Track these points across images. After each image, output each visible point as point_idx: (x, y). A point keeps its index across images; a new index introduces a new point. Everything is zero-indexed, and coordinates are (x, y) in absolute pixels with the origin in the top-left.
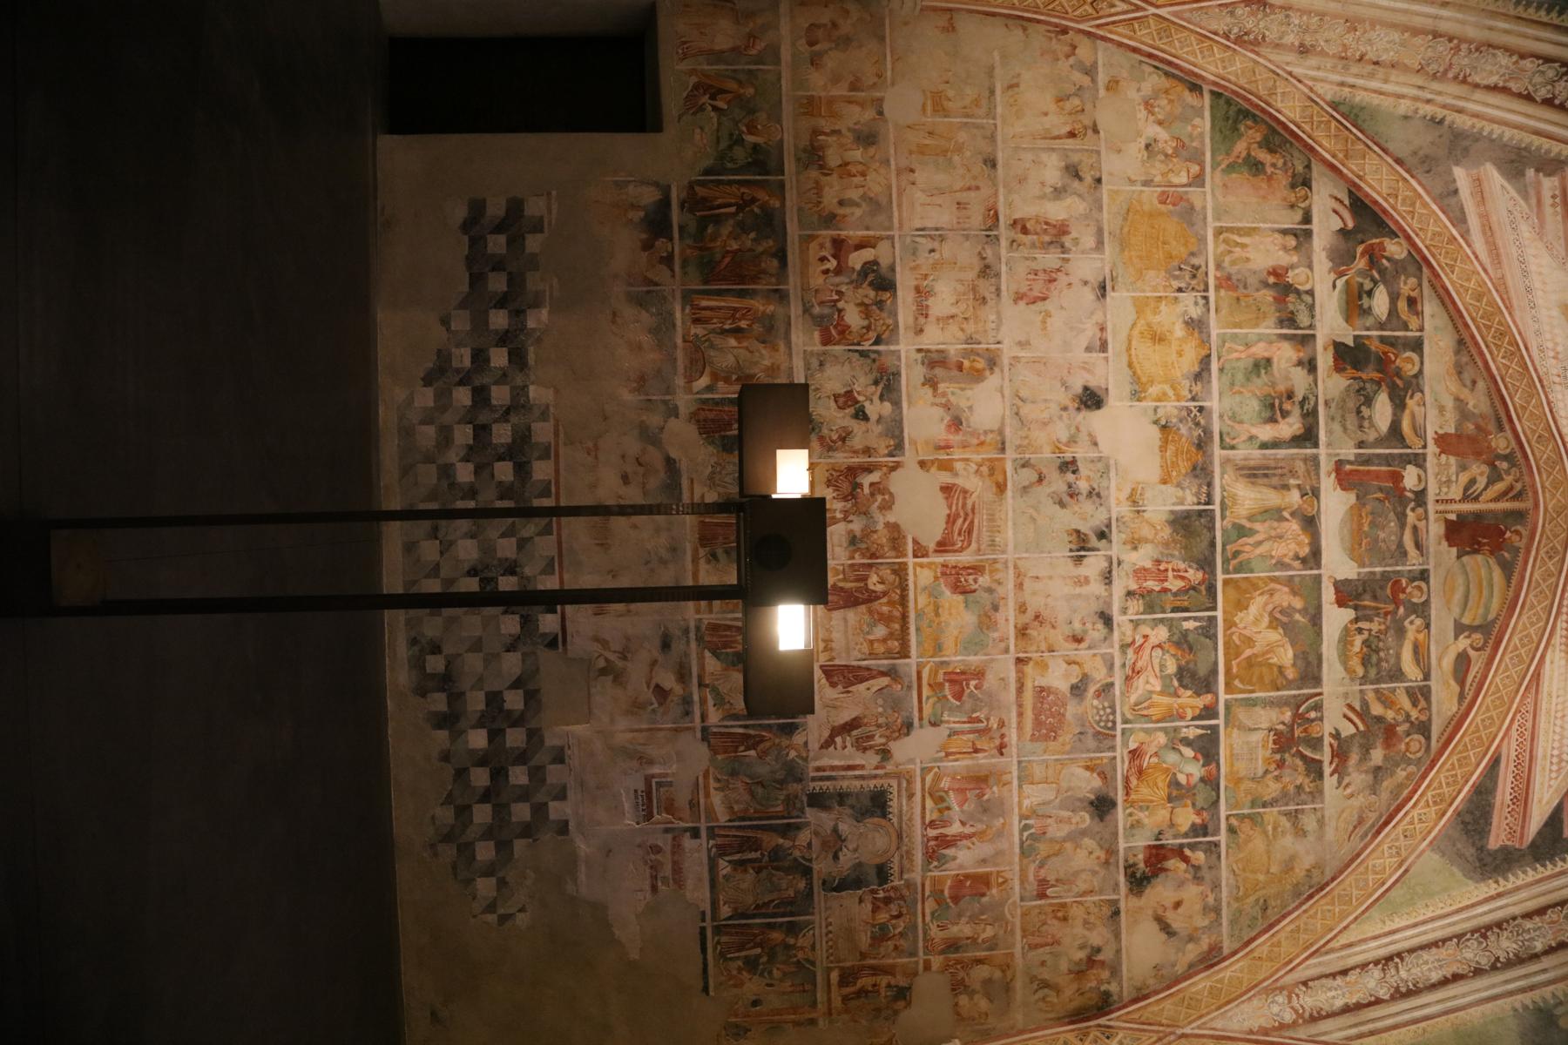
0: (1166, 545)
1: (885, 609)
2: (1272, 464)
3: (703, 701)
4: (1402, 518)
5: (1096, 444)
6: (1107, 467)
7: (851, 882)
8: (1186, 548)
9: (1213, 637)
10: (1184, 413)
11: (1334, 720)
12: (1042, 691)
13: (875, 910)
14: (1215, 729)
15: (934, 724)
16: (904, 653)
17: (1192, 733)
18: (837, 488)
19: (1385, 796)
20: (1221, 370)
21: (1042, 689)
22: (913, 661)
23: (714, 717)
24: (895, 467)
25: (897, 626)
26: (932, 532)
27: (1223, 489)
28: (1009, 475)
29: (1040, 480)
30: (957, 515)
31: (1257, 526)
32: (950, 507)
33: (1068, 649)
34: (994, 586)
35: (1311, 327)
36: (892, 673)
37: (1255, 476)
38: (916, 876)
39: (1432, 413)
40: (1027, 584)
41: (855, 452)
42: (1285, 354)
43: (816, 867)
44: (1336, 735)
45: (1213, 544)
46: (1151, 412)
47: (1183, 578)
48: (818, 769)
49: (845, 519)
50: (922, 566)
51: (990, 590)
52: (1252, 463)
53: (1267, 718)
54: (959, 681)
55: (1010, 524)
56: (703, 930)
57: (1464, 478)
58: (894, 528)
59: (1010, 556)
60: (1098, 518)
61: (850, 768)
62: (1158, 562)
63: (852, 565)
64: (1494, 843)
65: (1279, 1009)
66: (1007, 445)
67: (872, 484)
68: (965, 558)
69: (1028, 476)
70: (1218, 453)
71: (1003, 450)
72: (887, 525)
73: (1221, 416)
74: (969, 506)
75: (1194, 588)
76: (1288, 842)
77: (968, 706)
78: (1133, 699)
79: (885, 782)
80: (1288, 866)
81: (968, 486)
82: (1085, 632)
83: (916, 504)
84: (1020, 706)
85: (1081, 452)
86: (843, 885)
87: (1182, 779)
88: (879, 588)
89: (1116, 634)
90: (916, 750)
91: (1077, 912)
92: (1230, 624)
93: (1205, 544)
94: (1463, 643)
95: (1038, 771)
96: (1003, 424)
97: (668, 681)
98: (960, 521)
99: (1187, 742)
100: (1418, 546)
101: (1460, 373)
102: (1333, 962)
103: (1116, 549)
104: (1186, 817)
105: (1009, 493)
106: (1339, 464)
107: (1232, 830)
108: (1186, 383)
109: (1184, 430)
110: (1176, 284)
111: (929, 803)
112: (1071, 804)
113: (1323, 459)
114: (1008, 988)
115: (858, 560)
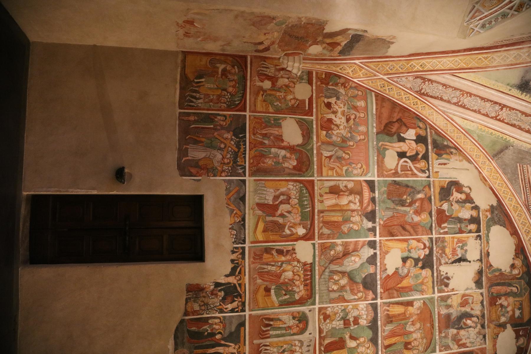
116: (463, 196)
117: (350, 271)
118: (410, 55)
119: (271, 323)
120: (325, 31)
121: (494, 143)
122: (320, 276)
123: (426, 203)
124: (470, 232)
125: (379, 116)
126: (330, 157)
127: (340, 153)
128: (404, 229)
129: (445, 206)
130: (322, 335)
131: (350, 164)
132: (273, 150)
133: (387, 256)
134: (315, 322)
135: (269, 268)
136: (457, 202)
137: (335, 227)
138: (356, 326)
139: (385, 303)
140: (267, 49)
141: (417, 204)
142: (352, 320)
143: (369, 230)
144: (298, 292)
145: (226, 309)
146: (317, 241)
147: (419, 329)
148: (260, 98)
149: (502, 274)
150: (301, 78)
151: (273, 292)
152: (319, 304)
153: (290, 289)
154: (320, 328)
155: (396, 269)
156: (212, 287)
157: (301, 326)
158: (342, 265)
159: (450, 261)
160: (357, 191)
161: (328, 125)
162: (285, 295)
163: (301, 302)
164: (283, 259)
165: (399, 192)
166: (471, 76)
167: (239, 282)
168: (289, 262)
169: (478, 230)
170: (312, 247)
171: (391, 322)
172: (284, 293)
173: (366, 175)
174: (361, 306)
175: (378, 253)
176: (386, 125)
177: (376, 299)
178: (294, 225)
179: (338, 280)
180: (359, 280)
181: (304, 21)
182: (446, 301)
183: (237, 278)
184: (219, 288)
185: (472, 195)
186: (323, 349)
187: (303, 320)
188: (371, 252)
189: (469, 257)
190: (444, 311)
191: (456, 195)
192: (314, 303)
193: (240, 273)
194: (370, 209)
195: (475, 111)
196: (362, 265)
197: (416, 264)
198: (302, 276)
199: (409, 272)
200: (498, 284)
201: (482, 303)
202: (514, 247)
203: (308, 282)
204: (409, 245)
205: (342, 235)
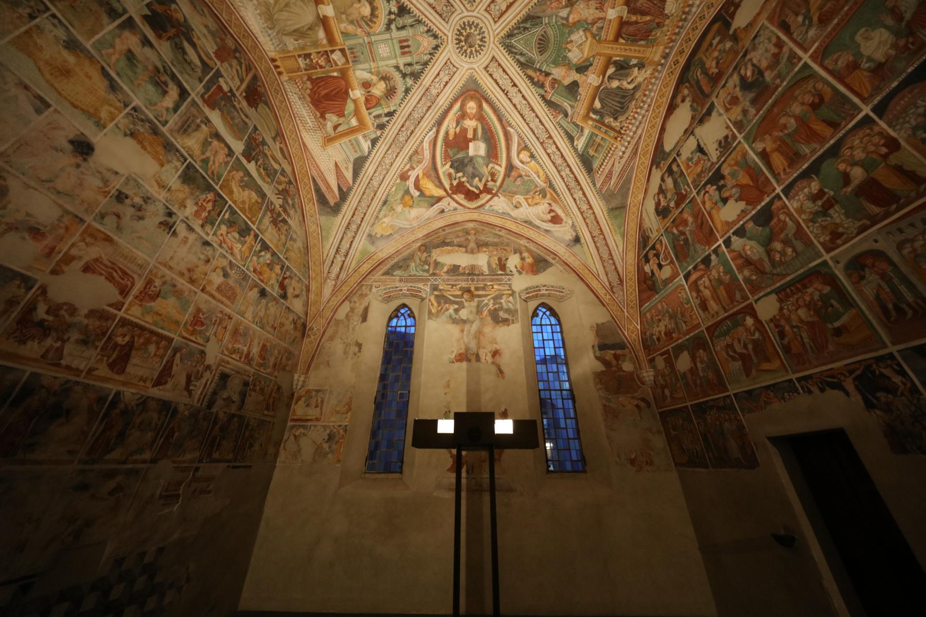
0: (192, 194)
1: (142, 340)
2: (185, 118)
3: (135, 462)
4: (234, 107)
5: (117, 173)
6: (135, 181)
7: (243, 395)
8: (198, 188)
9: (236, 212)
10: (131, 118)
11: (278, 202)
12: (219, 289)
13: (255, 391)
14: (261, 239)
15: (208, 341)
16: (171, 340)
17: (258, 248)
18: (33, 338)
19: (299, 210)
20: (118, 74)
21: (218, 288)
22: (176, 338)
23: (147, 455)
24: (44, 290)
25: (154, 338)
26: (111, 292)
27: (184, 148)
28: (102, 229)
29: (118, 216)
30: (110, 275)
31: (208, 154)
32: (101, 274)
33: (208, 268)
34: (163, 280)
35: (125, 11)
36: (176, 350)
37: (185, 131)
38: (253, 370)
39: (204, 40)
40: (172, 264)
41: (5, 312)
42: (131, 41)
43: (233, 412)
44: (281, 207)
45: (203, 177)
46: (117, 130)
47: (209, 201)
48: (198, 401)
49: (64, 341)
50: (128, 309)
51: (164, 283)
52: (179, 124)
53: (267, 221)
54: (197, 321)
55: (134, 250)
56: (234, 467)
57: (235, 72)
58: (92, 313)
59: (152, 262)
60: (162, 211)
61: (206, 384)
62: (196, 204)
63: (102, 349)
64: (332, 204)
65: (330, 283)
66: (81, 215)
67: (48, 312)
68: (139, 285)
69: (110, 221)
70: (164, 130)
71: (82, 221)
72: (87, 316)
73: (146, 107)
74: (109, 264)
75: (215, 201)
76: (296, 246)
77: (208, 322)
78: (239, 257)
79: (219, 371)
80: (300, 251)
81: (94, 256)
82: (207, 256)
83: (85, 292)
84: (219, 301)
85: (117, 184)
86: (243, 402)
87: (268, 262)
88: (127, 339)
89: (215, 245)
90: (213, 353)
91: (283, 320)
92: (235, 202)
93: (201, 180)
94: (278, 143)
95: (243, 308)
96: (61, 206)
97: (112, 484)
98: (115, 274)
99: (260, 251)
100: (247, 116)
101: (195, 7)
102: (328, 262)
103: (181, 214)
104: (277, 269)
105: (115, 238)
106: (202, 96)
107: (287, 259)
108: (112, 97)
109: (142, 130)
110: (25, 11)
111: (234, 356)
112: (258, 303)
113: (196, 99)
114: (290, 353)
115: (100, 344)
116: (661, 196)
117: (763, 246)
118: (604, 306)
119: (890, 306)
120: (603, 368)
121: (616, 217)
122: (785, 276)
123: (678, 221)
124: (678, 166)
125: (649, 298)
126: (685, 322)
127: (679, 316)
128: (702, 224)
129: (672, 204)
130: (868, 223)
131: (682, 303)
132: (701, 375)
133: (730, 220)
134: (853, 247)
135: (806, 340)
136: (666, 198)
137: (732, 287)
138: (826, 190)
139: (778, 181)
140: (643, 400)
141: (681, 228)
142: (820, 203)
143: (717, 255)
144: (820, 291)
145: (905, 384)
146: (752, 299)
147: (787, 114)
148: (675, 395)
149: (693, 101)
150: (654, 367)
151: (837, 324)
152: (823, 256)
153: (820, 303)
154: (858, 234)
155: (736, 201)
156: (879, 412)
157: (869, 262)
158: (761, 259)
159: (706, 158)
160: (695, 287)
161: (668, 334)
162: (832, 306)
163: (831, 280)
164: (787, 328)
165: (682, 250)
166: (592, 266)
167: (848, 375)
168: (788, 320)
169: (675, 160)
170: (759, 303)
171: (797, 154)
172: (830, 309)
173: (683, 286)
174: (795, 205)
175: (732, 231)
176: (651, 290)
177: (778, 197)
178: (747, 330)
179: (779, 252)
180: (767, 230)
181: (599, 386)
182: (741, 121)
183: (843, 378)
184: (875, 401)
185: (656, 190)
186: (894, 207)
187: (857, 265)
188: (734, 238)
189: (695, 146)
190: (752, 111)
191: (663, 203)
192: (825, 263)
193: (833, 377)
194: (702, 267)
195: (608, 246)
196: (750, 239)
197: (724, 186)
198: (796, 296)
199: (733, 187)
200: (702, 92)
201: (724, 86)
202: (672, 117)
203: (799, 286)
204: (712, 208)
205: (734, 278)
